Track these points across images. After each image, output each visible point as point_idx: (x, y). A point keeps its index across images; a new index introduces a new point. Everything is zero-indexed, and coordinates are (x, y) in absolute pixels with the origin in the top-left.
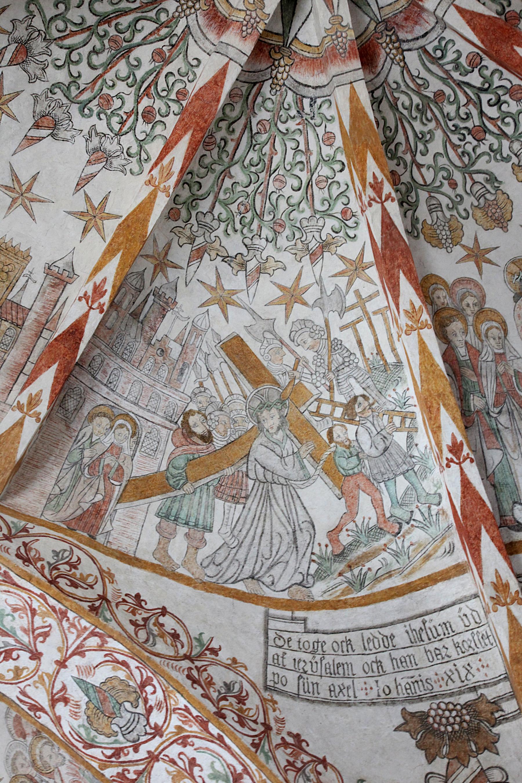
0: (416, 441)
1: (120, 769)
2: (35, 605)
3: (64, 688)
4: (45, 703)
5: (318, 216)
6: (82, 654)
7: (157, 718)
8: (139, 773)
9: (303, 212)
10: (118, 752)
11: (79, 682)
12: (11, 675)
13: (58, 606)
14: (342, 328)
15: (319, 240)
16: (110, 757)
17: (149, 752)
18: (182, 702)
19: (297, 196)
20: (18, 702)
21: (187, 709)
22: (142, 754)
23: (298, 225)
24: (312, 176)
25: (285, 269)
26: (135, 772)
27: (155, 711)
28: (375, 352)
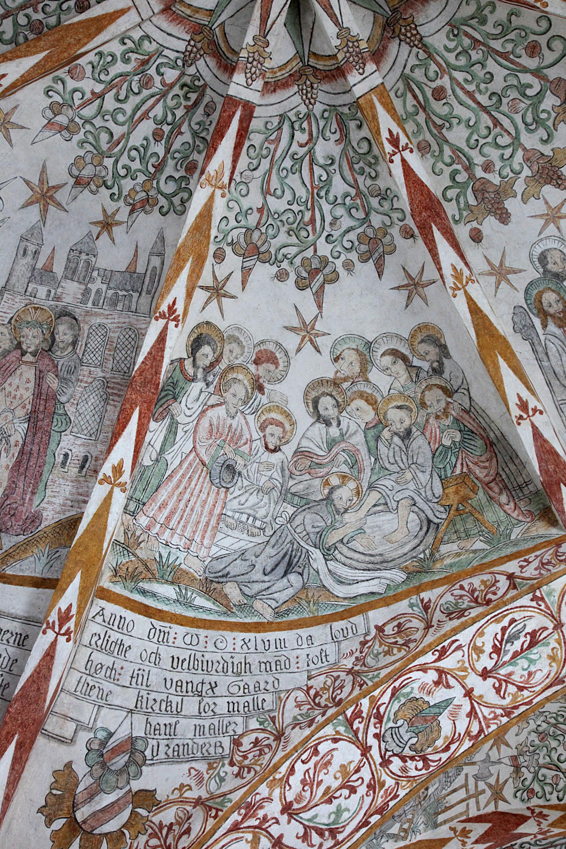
0: (390, 841)
1: (364, 715)
2: (526, 693)
3: (448, 686)
4: (444, 664)
5: (536, 768)
6: (469, 715)
7: (396, 764)
8: (356, 733)
9: (544, 758)
10: (380, 718)
11: (448, 702)
12: (479, 644)
13: (517, 712)
14: (467, 775)
15: (523, 765)
16: (378, 709)
17: (371, 747)
18: (402, 793)
19: (555, 756)
20: (454, 638)
21: (396, 796)
22: (372, 741)
23: (537, 752)
24: (563, 773)
25: (516, 735)
26: (358, 729)
27: (401, 764)
28: (448, 805)
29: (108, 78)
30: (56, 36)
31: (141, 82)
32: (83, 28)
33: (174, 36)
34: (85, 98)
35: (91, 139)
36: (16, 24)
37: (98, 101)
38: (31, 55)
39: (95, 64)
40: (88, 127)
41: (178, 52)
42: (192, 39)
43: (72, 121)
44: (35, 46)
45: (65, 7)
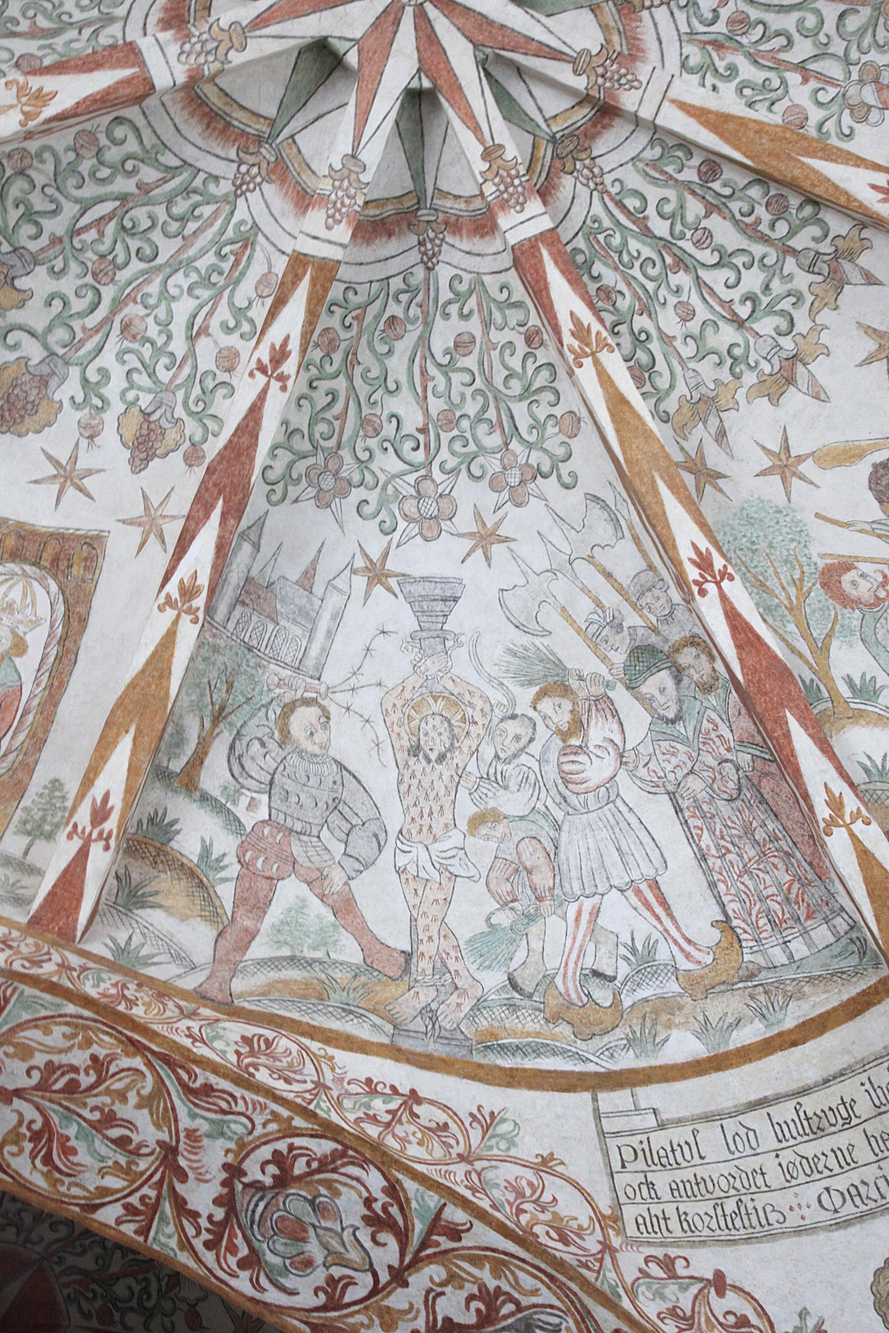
29: (771, 75)
30: (774, 163)
31: (745, 30)
32: (739, 139)
33: (658, 34)
34: (820, 86)
35: (867, 40)
36: (792, 232)
37: (811, 66)
38: (821, 174)
39: (767, 104)
40: (854, 55)
41: (672, 14)
42: (643, 7)
43: (861, 81)
44: (807, 177)
45: (727, 191)
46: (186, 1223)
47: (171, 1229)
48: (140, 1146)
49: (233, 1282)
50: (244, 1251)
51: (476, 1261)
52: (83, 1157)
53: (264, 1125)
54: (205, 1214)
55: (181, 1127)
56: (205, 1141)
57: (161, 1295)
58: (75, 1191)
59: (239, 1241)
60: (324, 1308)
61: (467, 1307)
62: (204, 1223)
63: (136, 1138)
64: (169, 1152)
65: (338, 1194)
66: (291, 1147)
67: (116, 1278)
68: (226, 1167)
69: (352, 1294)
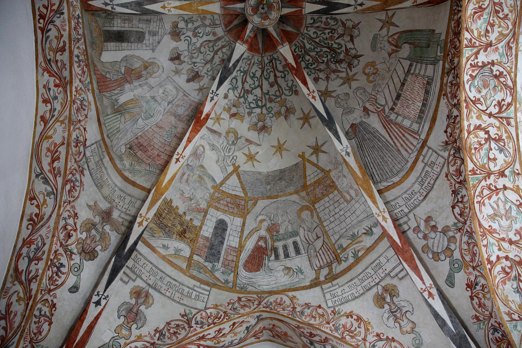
46: (474, 56)
47: (470, 53)
48: (488, 36)
49: (465, 75)
50: (474, 74)
51: (506, 131)
52: (479, 22)
53: (508, 66)
54: (478, 60)
55: (498, 45)
56: (497, 53)
57: (314, 68)
58: (469, 23)
59: (476, 72)
60: (472, 101)
61: (495, 134)
62: (476, 61)
63: (490, 34)
64: (490, 45)
65: (501, 92)
66: (506, 75)
67: (309, 55)
68: (493, 61)
69: (479, 106)
